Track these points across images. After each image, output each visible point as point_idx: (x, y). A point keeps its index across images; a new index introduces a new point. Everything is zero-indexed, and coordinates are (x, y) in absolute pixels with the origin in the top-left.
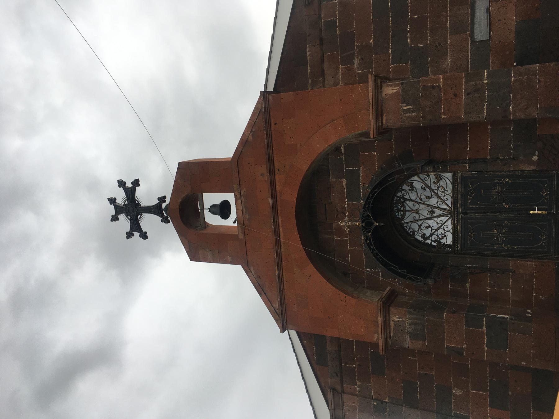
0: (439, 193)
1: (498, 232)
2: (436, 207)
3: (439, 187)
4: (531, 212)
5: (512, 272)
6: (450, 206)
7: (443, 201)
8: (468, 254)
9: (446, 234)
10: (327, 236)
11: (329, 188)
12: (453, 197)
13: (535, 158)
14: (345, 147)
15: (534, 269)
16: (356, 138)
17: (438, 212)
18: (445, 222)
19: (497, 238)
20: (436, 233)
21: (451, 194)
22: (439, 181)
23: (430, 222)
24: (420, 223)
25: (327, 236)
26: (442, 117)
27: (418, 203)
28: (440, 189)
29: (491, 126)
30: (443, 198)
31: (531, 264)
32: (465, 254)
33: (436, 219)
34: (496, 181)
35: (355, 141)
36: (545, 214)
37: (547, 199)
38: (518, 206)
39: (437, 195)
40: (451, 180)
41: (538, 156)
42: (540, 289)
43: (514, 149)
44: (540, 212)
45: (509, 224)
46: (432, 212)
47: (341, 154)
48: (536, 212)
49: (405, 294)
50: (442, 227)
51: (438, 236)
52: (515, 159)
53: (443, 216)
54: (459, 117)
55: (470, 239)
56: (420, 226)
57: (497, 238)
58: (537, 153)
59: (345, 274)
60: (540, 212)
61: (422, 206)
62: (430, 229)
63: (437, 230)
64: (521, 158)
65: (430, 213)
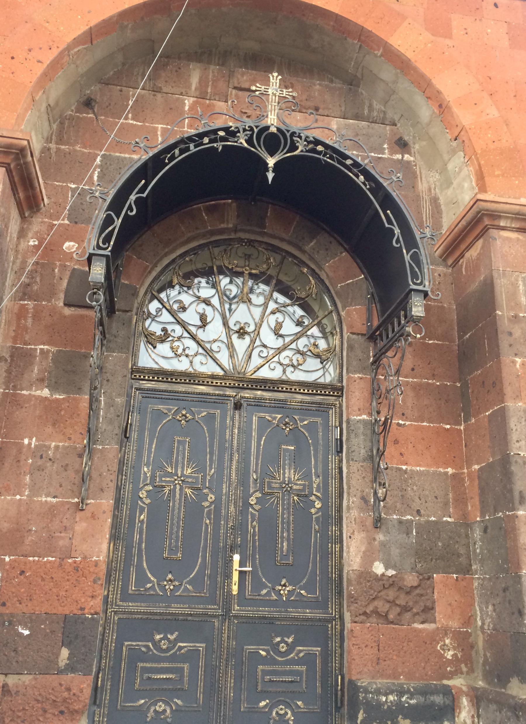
0: (287, 353)
1: (188, 477)
2: (253, 341)
3: (302, 354)
4: (236, 558)
5: (78, 503)
6: (254, 375)
7: (268, 360)
8: (128, 402)
9: (183, 358)
10: (195, 81)
11: (317, 109)
12: (282, 382)
13: (379, 568)
14: (409, 162)
15: (85, 558)
16: (430, 190)
17: (241, 345)
18: (215, 360)
19: (170, 475)
20: (186, 334)
21: (284, 377)
22: (317, 356)
23: (215, 330)
24: (215, 301)
25: (195, 81)
26: (519, 360)
27: (265, 305)
28: (298, 356)
29: (454, 475)
30: (276, 359)
31: (99, 550)
32: (129, 396)
33: (224, 338)
34: (316, 481)
35: (422, 186)
36: (230, 590)
37: (268, 594)
38: (254, 528)
39: (285, 347)
40: (319, 381)
41: (383, 575)
42: (22, 572)
43: (400, 522)
44: (235, 577)
45: (206, 504)
46: (242, 333)
47: (392, 153)
48: (236, 565)
49: (22, 234)
50: (201, 351)
51: (179, 338)
52: (378, 523)
53: (231, 356)
54: (518, 397)
55: (170, 410)
56: (207, 302)
57: (170, 475)
58: (391, 572)
59: (88, 104)
60: (235, 577)
61: (257, 312)
62: (199, 323)
63: (193, 337)
64: (380, 537)
65: (241, 328)
